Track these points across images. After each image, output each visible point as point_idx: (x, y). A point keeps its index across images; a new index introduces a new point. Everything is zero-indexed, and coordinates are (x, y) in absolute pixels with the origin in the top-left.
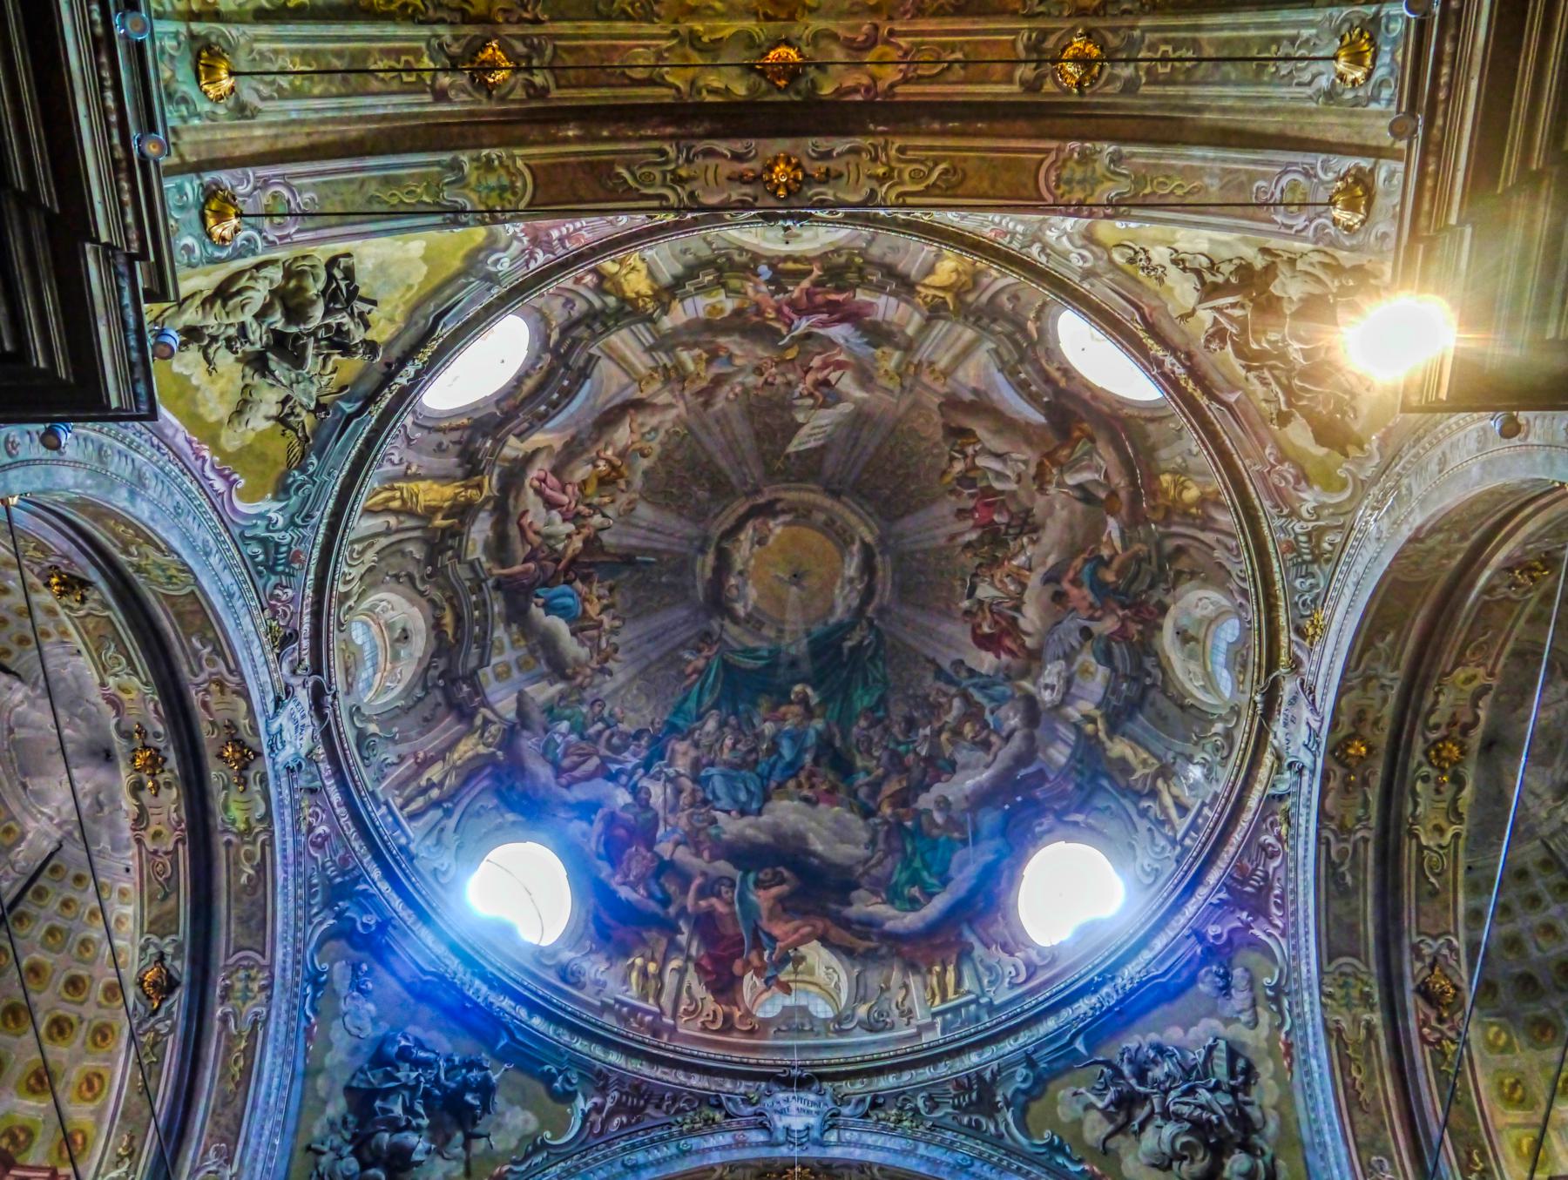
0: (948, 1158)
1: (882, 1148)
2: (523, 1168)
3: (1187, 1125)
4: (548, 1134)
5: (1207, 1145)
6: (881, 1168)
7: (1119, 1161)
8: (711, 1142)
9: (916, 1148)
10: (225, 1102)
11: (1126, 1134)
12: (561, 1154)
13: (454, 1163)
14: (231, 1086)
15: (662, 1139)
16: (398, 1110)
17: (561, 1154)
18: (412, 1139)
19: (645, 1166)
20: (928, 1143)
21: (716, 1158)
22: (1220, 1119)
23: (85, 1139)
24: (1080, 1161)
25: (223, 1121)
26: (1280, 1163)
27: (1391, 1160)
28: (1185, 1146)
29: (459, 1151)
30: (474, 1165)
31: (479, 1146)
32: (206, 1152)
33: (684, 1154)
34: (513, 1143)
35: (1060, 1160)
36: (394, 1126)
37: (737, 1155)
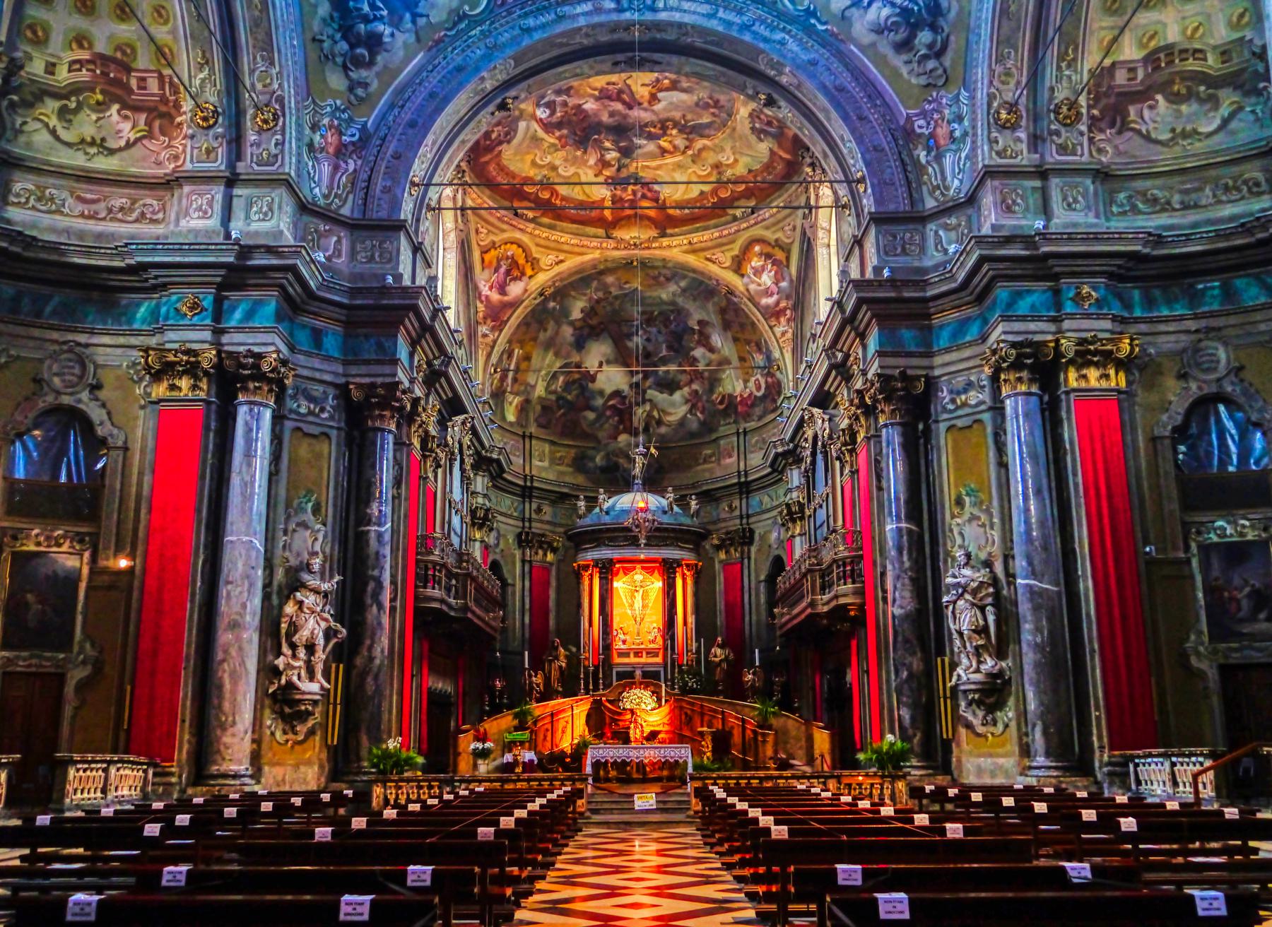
0: (737, 20)
1: (694, 13)
2: (453, 32)
3: (898, 10)
4: (467, 8)
5: (908, 23)
6: (693, 27)
7: (851, 25)
8: (579, 10)
9: (717, 11)
10: (256, 23)
11: (858, 8)
12: (476, 21)
13: (407, 35)
14: (257, 13)
15: (545, 8)
16: (366, 8)
17: (476, 21)
18: (381, 27)
19: (536, 29)
20: (725, 8)
21: (582, 21)
22: (919, 10)
23: (170, 50)
24: (825, 23)
25: (260, 37)
26: (952, 38)
27: (1016, 52)
28: (893, 23)
29: (409, 25)
30: (421, 33)
31: (422, 22)
32: (255, 58)
33: (561, 18)
34: (444, 16)
35: (813, 21)
36: (366, 19)
37: (596, 19)
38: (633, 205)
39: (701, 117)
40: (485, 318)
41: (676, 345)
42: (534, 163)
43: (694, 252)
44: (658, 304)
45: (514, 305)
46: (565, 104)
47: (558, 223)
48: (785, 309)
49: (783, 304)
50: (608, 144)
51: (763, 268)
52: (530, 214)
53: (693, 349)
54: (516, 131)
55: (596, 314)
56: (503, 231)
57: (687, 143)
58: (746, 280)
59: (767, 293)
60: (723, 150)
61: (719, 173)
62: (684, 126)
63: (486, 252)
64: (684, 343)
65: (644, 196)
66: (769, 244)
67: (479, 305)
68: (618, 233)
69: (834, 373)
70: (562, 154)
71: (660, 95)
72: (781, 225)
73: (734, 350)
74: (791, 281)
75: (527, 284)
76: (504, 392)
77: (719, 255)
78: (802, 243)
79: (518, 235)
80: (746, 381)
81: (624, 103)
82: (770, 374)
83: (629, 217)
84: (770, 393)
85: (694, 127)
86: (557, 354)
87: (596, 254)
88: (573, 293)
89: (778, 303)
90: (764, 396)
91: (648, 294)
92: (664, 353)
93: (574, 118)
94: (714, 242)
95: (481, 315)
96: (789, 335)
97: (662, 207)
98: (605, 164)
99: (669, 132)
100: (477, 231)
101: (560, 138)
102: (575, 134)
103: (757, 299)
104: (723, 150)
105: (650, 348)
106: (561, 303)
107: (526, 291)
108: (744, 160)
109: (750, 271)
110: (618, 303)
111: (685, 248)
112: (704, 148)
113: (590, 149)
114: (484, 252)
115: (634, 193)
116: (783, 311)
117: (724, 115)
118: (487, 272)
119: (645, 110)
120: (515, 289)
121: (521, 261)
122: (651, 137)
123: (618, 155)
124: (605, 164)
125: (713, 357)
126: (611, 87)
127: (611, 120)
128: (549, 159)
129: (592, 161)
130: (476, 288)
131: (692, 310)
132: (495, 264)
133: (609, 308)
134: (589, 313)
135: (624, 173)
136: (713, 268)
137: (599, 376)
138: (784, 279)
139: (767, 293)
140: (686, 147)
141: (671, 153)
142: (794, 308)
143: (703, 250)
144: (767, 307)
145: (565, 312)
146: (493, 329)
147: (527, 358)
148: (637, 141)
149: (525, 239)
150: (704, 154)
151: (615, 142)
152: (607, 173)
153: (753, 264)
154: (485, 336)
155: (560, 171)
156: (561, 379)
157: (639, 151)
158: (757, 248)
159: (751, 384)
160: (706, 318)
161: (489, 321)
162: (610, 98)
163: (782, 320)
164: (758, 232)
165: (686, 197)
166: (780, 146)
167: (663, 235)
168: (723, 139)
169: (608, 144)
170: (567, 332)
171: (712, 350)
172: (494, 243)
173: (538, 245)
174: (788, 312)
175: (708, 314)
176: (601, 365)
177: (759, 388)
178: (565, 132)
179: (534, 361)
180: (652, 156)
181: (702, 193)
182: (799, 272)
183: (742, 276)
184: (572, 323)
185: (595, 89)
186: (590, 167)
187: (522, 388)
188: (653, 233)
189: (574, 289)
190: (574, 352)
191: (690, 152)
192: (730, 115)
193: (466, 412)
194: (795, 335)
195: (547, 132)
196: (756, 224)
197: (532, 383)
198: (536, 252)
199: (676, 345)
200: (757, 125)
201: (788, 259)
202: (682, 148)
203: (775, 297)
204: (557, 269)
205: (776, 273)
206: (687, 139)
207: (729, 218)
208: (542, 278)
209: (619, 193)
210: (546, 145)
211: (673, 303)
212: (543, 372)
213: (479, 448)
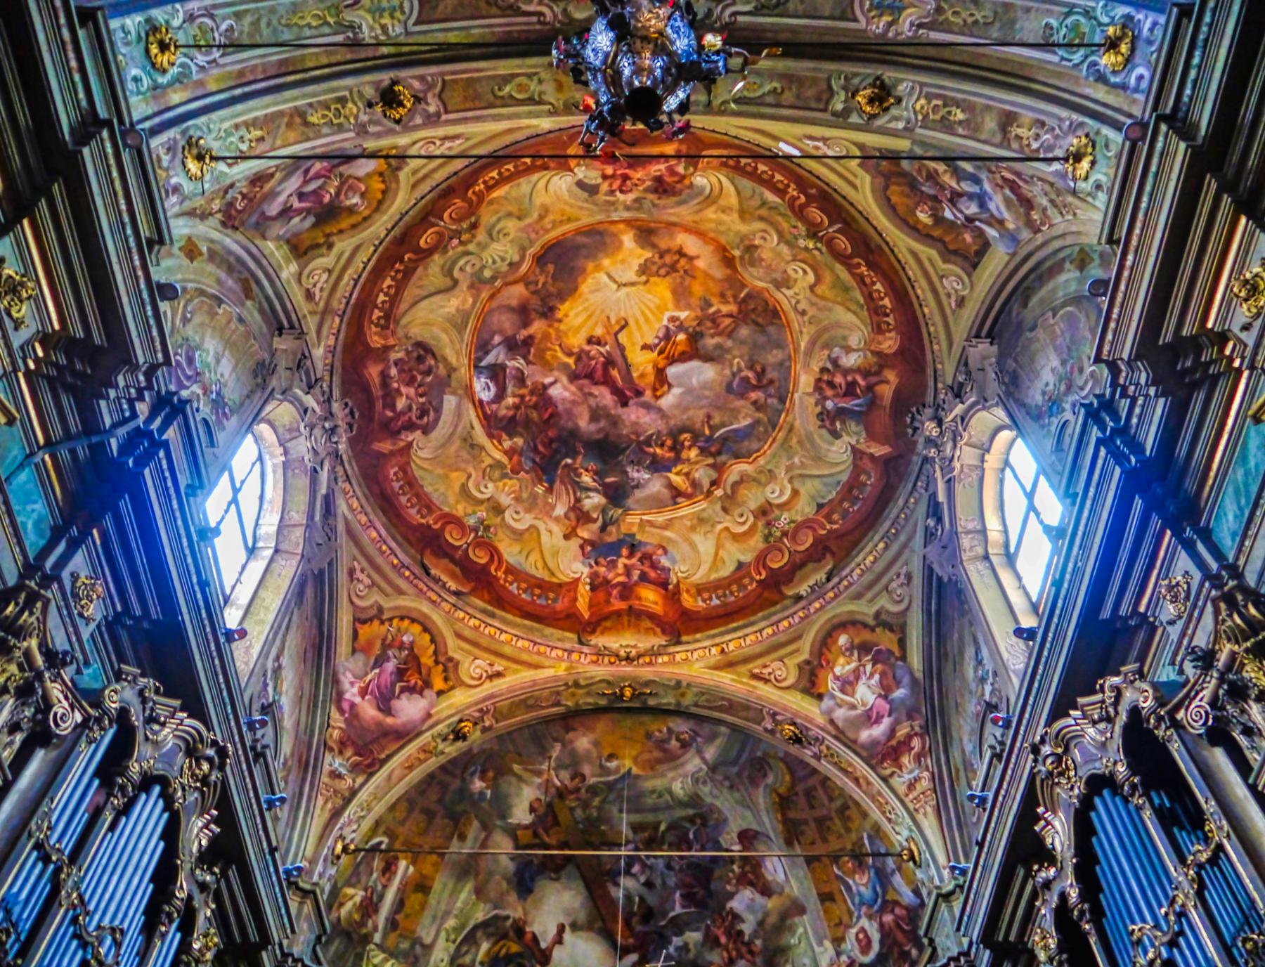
38: (627, 591)
39: (735, 413)
40: (343, 744)
41: (702, 894)
42: (464, 489)
43: (730, 665)
44: (668, 807)
45: (403, 735)
46: (521, 379)
47: (498, 612)
48: (909, 737)
49: (902, 732)
50: (587, 479)
51: (857, 674)
52: (452, 585)
53: (731, 896)
54: (438, 411)
55: (556, 823)
56: (400, 592)
57: (714, 475)
58: (827, 703)
59: (870, 718)
60: (771, 475)
61: (769, 524)
62: (709, 439)
63: (364, 622)
64: (713, 886)
65: (644, 578)
66: (865, 626)
67: (335, 714)
68: (599, 640)
69: (1138, 503)
70: (512, 484)
71: (672, 371)
72: (884, 581)
73: (809, 884)
74: (914, 681)
75: (432, 705)
76: (367, 939)
77: (775, 667)
78: (927, 600)
79: (425, 608)
80: (838, 941)
81: (616, 391)
82: (889, 906)
83: (618, 614)
84: (896, 943)
85: (725, 439)
86: (479, 892)
87: (560, 670)
88: (516, 767)
89: (892, 731)
90: (881, 958)
91: (649, 784)
92: (678, 909)
93: (534, 415)
94: (765, 645)
95: (336, 733)
96: (925, 784)
97: (672, 594)
98: (582, 517)
99: (684, 455)
100: (351, 572)
101: (510, 453)
102: (535, 450)
103: (851, 735)
104: (771, 475)
105: (652, 900)
106: (494, 785)
107: (429, 716)
108: (808, 489)
109: (832, 685)
110: (596, 802)
111: (712, 661)
112: (743, 480)
113: (557, 485)
114: (360, 620)
115: (628, 570)
116: (905, 744)
117: (773, 401)
118: (360, 657)
119: (647, 407)
120: (409, 708)
121: (427, 660)
122: (657, 466)
123: (603, 500)
124: (582, 517)
125: (771, 903)
126: (594, 350)
127: (593, 427)
128: (490, 490)
129: (560, 510)
130: (336, 681)
131: (728, 814)
132: (377, 649)
133: (579, 813)
134: (546, 815)
135: (612, 536)
136: (766, 692)
137: (557, 953)
138: (898, 684)
139: (870, 718)
140: (714, 483)
141: (688, 496)
142: (926, 730)
143: (747, 660)
144: (874, 743)
145: (501, 806)
146: (355, 768)
147: (422, 886)
148: (636, 474)
149: (437, 618)
150: (743, 491)
151: (599, 475)
152: (584, 533)
153: (838, 670)
154: (335, 775)
155: (507, 515)
156: (485, 946)
157: (638, 494)
158: (843, 640)
159: (850, 945)
160: (755, 827)
161: (349, 753)
162: (590, 376)
163: (905, 760)
164: (845, 608)
165: (714, 576)
166: (872, 436)
167: (679, 643)
168: (774, 456)
169: (587, 479)
170: (503, 847)
171: (767, 890)
172: (381, 610)
173: (459, 636)
174: (916, 743)
175: (757, 815)
176: (561, 929)
177: (866, 947)
178: (519, 441)
179: (432, 900)
180: (657, 504)
181: (740, 565)
182: (927, 659)
183: (820, 697)
184: (512, 832)
185: (569, 354)
186: (557, 519)
187: (405, 945)
188: (658, 640)
189: (521, 758)
190: (512, 897)
191: (719, 493)
192: (782, 400)
193: (209, 727)
194: (936, 779)
195: (490, 436)
196: (836, 596)
197: (428, 940)
198: (453, 647)
199: (702, 894)
200: (829, 404)
201: (902, 643)
202: (706, 484)
203: (886, 722)
204: (489, 688)
205: (883, 675)
206: (713, 466)
207: (788, 602)
208: (460, 698)
209: (602, 570)
210: (488, 461)
211: (694, 800)
212: (451, 923)
213: (253, 935)
